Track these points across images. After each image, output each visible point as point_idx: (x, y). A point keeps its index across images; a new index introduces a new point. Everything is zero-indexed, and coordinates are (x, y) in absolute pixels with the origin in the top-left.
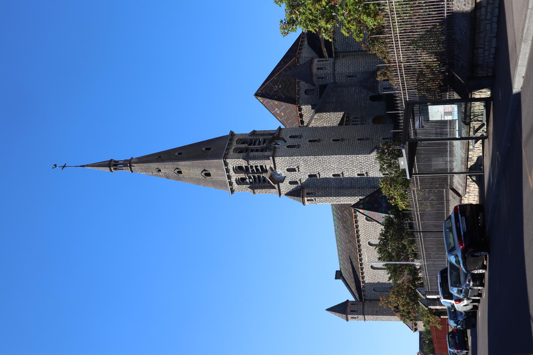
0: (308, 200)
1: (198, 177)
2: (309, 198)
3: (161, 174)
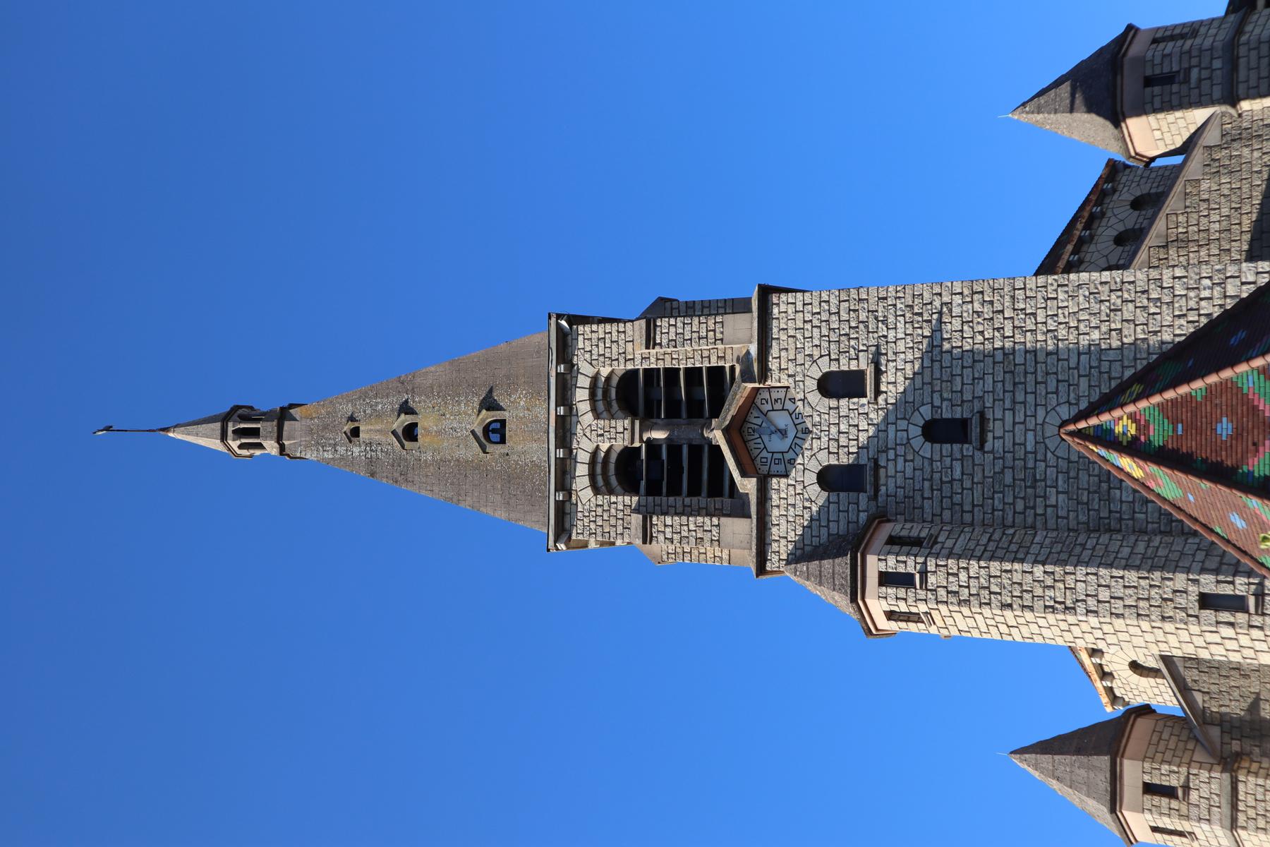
0: (886, 579)
1: (462, 453)
2: (892, 564)
3: (356, 450)
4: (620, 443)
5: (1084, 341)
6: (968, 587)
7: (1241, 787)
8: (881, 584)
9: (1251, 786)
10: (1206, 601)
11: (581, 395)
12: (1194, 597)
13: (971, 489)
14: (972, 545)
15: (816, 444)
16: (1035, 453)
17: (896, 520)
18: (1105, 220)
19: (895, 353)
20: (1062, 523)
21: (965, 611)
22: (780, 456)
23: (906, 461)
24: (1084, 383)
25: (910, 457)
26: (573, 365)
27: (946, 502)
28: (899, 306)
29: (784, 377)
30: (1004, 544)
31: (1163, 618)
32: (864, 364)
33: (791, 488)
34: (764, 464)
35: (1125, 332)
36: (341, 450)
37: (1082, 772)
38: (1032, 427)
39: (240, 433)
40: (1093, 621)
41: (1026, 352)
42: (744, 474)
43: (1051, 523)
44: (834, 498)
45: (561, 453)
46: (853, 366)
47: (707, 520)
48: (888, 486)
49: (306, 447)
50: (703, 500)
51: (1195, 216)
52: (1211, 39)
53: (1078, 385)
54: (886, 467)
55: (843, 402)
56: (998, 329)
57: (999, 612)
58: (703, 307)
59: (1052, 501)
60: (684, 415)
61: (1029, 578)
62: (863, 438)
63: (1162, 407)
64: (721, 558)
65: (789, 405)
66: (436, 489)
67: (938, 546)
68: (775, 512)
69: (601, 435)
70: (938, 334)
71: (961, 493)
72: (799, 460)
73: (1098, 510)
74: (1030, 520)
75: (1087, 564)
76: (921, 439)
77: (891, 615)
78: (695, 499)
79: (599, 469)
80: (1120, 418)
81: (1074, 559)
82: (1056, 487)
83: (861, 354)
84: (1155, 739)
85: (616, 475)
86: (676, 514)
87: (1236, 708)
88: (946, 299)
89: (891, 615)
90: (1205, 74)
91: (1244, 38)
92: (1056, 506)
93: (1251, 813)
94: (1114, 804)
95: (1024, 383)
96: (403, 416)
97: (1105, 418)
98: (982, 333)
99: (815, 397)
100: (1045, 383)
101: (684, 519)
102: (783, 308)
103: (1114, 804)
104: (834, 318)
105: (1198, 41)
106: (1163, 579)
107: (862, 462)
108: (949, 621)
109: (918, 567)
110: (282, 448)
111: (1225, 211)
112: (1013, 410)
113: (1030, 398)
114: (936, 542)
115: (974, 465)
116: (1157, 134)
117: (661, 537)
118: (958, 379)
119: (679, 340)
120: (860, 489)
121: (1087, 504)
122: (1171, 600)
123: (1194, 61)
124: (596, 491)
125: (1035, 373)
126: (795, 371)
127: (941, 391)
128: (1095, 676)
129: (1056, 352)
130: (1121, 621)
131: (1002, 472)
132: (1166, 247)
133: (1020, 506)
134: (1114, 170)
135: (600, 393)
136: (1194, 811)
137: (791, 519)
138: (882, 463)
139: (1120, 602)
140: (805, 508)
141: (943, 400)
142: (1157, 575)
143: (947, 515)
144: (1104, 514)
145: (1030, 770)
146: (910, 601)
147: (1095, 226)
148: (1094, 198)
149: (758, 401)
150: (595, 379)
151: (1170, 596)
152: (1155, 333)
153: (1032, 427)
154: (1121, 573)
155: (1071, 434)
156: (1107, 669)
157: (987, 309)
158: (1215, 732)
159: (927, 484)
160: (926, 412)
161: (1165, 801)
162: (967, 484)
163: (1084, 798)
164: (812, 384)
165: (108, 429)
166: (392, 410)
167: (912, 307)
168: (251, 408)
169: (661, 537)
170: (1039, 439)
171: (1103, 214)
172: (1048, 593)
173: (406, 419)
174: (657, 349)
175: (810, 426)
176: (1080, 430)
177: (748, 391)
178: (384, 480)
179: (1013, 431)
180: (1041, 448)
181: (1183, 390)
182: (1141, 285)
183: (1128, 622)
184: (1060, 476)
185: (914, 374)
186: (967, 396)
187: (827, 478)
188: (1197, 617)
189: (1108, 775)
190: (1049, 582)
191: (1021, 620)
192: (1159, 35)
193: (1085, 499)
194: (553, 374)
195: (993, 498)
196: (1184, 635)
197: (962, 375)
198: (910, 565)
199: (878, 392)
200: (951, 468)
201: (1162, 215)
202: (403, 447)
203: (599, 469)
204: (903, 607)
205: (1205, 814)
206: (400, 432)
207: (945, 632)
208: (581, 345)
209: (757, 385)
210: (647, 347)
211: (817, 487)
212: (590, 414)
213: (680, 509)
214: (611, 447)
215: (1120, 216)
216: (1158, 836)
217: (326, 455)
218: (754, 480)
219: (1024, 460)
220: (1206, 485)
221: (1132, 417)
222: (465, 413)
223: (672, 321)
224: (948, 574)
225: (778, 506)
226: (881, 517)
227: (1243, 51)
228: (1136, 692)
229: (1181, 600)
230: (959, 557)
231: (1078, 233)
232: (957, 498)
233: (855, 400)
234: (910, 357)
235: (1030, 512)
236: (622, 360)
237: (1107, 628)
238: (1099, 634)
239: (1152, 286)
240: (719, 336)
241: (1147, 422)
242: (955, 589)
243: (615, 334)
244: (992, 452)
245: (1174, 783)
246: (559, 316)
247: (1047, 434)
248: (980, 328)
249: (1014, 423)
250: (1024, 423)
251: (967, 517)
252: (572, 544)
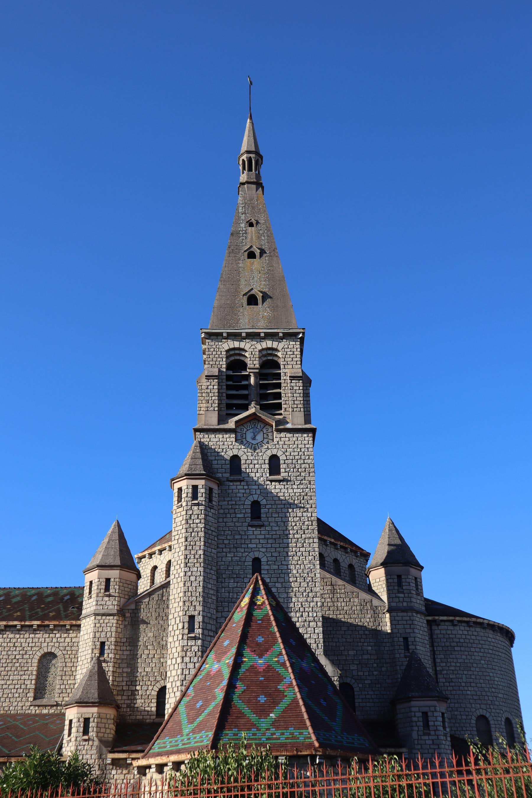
0: (195, 488)
1: (243, 282)
2: (201, 491)
3: (243, 225)
4: (248, 362)
5: (292, 567)
6: (193, 523)
7: (112, 617)
8: (193, 486)
9: (112, 621)
10: (192, 618)
11: (269, 344)
12: (193, 613)
13: (232, 522)
14: (210, 524)
15: (250, 454)
16: (248, 548)
17: (219, 489)
18: (344, 554)
19: (287, 488)
20: (220, 559)
21: (183, 522)
22: (244, 437)
23: (243, 493)
24: (276, 567)
25: (245, 495)
26: (282, 340)
27: (227, 511)
28: (307, 490)
29: (278, 439)
30: (211, 537)
31: (184, 602)
32: (283, 475)
33: (231, 443)
34: (241, 430)
35: (296, 583)
36: (243, 217)
37: (112, 553)
38: (258, 546)
39: (250, 160)
40: (182, 574)
41: (288, 544)
42: (236, 422)
43: (219, 555)
44: (228, 462)
45: (244, 335)
46: (282, 470)
47: (217, 405)
48: (233, 486)
49: (244, 197)
50: (225, 401)
51: (344, 596)
52: (415, 601)
53: (275, 565)
54: (240, 485)
55: (267, 466)
56: (297, 532)
57: (184, 536)
58: (307, 401)
59: (228, 555)
60: (261, 392)
61: (198, 548)
62: (252, 475)
63: (267, 615)
64: (200, 410)
65: (266, 441)
66: (226, 269)
67: (209, 510)
68: (221, 436)
69: (252, 352)
70: (295, 507)
71: (230, 517)
72: (243, 447)
73: (225, 574)
74: (220, 546)
75: (204, 572)
76: (252, 500)
77: (180, 490)
78: (225, 398)
79: (237, 352)
80: (263, 598)
81: (206, 566)
82: (234, 556)
83: (287, 473)
84: (128, 582)
85: (235, 360)
86: (218, 389)
87: (143, 615)
88: (310, 510)
89: (180, 490)
90: (401, 599)
91: (414, 614)
92: (226, 557)
93: (101, 621)
94: (101, 567)
95: (275, 543)
96: (259, 251)
97: (263, 592)
98: (296, 525)
99: (269, 453)
100: (276, 552)
101: (217, 394)
102: (307, 439)
103: (101, 567)
104: (302, 461)
105: (415, 596)
106: (200, 602)
107: (243, 474)
108: (179, 515)
109: (200, 502)
110: (243, 184)
111: (345, 608)
112: (265, 538)
113: (269, 546)
114: (211, 508)
115: (242, 522)
116: (378, 580)
117: (208, 384)
118: (277, 516)
119: (293, 391)
120: (231, 474)
121: (228, 569)
122: (192, 605)
123: (406, 595)
124: (227, 351)
125: (280, 547)
126: (280, 444)
127: (272, 508)
128: (150, 551)
129: (288, 556)
130: (182, 585)
131: (240, 534)
132: (331, 585)
133: (226, 542)
134: (366, 556)
135: (270, 352)
136: (100, 599)
137: (218, 443)
138: (242, 483)
139: (190, 585)
140: (223, 449)
141: (269, 509)
142: (201, 599)
143: (222, 511)
144: (224, 576)
145: (111, 530)
146: (186, 499)
147: (342, 550)
148: (354, 548)
149: (267, 427)
150: (276, 350)
151: (193, 604)
152: (295, 595)
153: (258, 546)
154: (201, 585)
155: (257, 578)
156: (153, 556)
157: (305, 527)
158: (133, 607)
159: (234, 503)
160: (264, 502)
161: (103, 587)
162: (234, 520)
163: (102, 553)
164: (274, 452)
165: (251, 83)
166: (262, 245)
167: (307, 495)
168: (262, 163)
169: (208, 384)
170: (253, 549)
171: (347, 553)
172: (192, 556)
173: (257, 252)
174: (289, 381)
175: (256, 451)
176: (258, 581)
177: (272, 423)
178: (229, 241)
179: (256, 539)
180: (249, 550)
181: (274, 623)
182: (314, 589)
183: (182, 588)
184: (238, 558)
185: (279, 497)
186: (270, 519)
187: (236, 459)
188: (186, 615)
189: (112, 564)
190: (197, 556)
191: (181, 545)
192: (418, 580)
193: (229, 568)
194: (279, 331)
195: (229, 531)
196: (178, 609)
197: (279, 517)
198: (201, 499)
199: (271, 481)
200: (241, 513)
201: (345, 583)
202: (245, 251)
203: (237, 352)
204: (184, 495)
205: (99, 603)
206: (252, 250)
207: (174, 512)
208: (291, 343)
209: (274, 428)
210: (290, 377)
211: (231, 455)
212: (261, 348)
213: (221, 391)
214: (247, 357)
215: (345, 560)
216: (88, 584)
217: (241, 208)
218: (234, 427)
219: (245, 543)
220: (239, 631)
221: (264, 603)
222: (260, 284)
223: (301, 388)
224: (198, 515)
225: (223, 437)
226: (220, 483)
227: (410, 614)
228: (144, 568)
229: (192, 609)
230: (205, 519)
231: (339, 543)
232: (228, 516)
233: (268, 471)
234: (286, 495)
235: (223, 546)
236: (285, 363)
237: (179, 579)
238: (177, 576)
239: (314, 594)
240: (295, 409)
241: (262, 609)
242: (192, 518)
243: (296, 359)
244: (248, 530)
245: (111, 591)
246: (303, 333)
247: (255, 553)
248: (298, 524)
249: (259, 539)
250: (260, 543)
251: (221, 520)
252: (204, 339)
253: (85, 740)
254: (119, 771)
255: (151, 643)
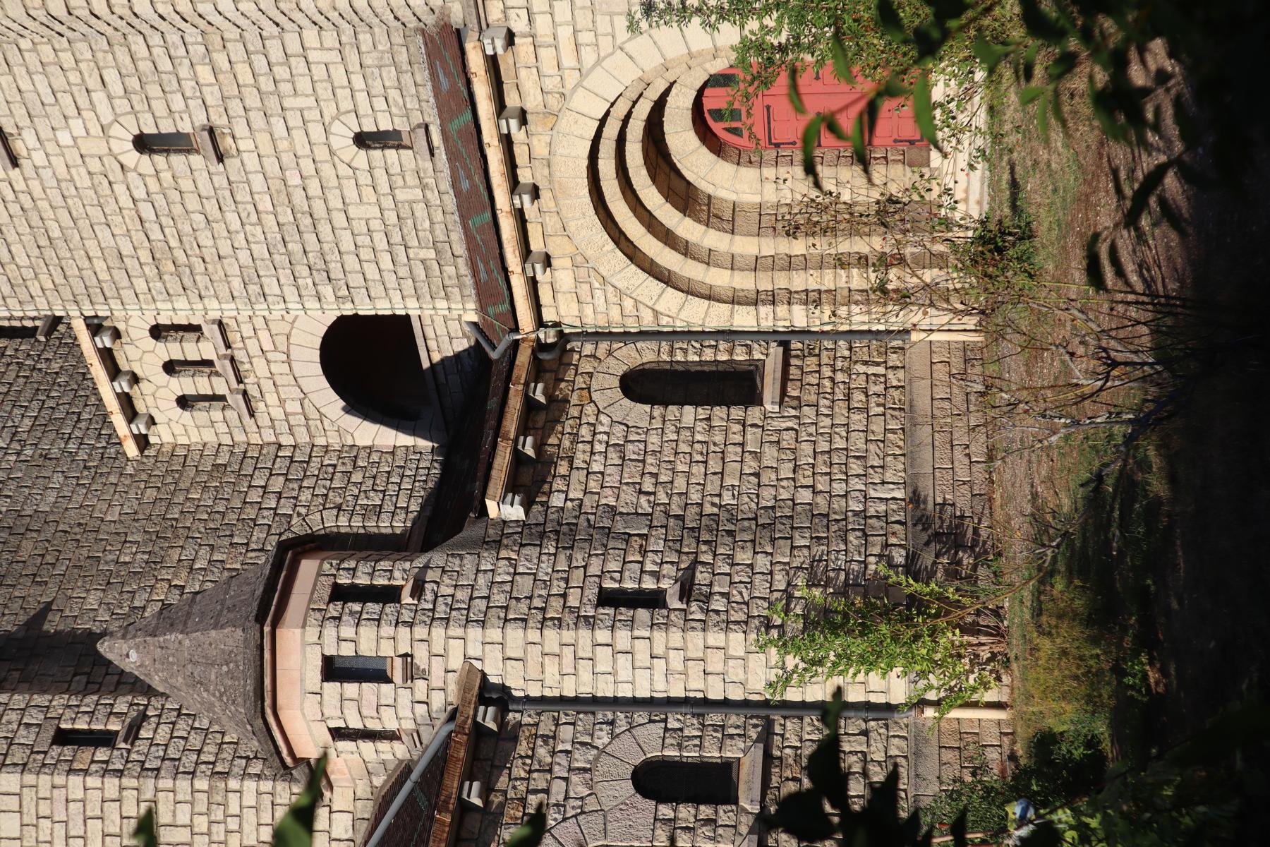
253: (418, 591)
254: (559, 484)
255: (126, 596)
